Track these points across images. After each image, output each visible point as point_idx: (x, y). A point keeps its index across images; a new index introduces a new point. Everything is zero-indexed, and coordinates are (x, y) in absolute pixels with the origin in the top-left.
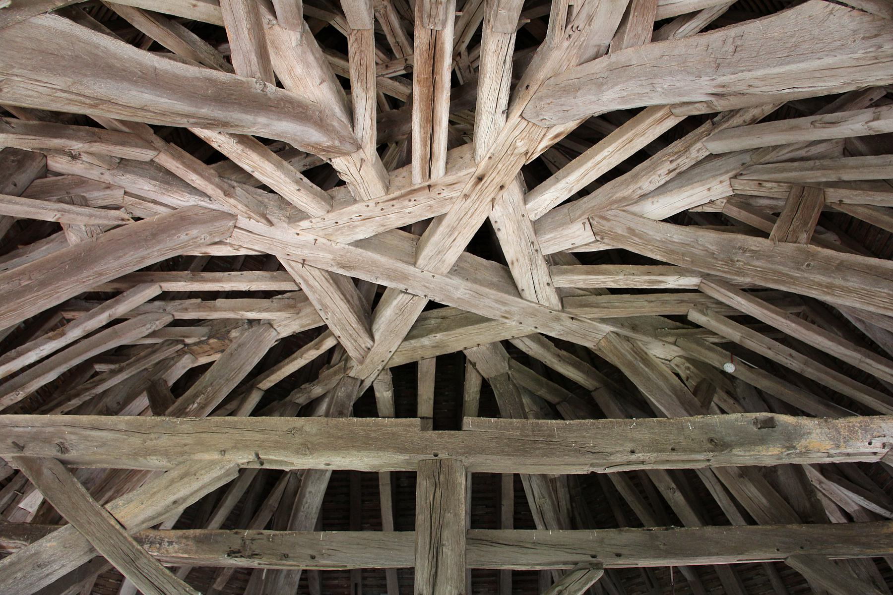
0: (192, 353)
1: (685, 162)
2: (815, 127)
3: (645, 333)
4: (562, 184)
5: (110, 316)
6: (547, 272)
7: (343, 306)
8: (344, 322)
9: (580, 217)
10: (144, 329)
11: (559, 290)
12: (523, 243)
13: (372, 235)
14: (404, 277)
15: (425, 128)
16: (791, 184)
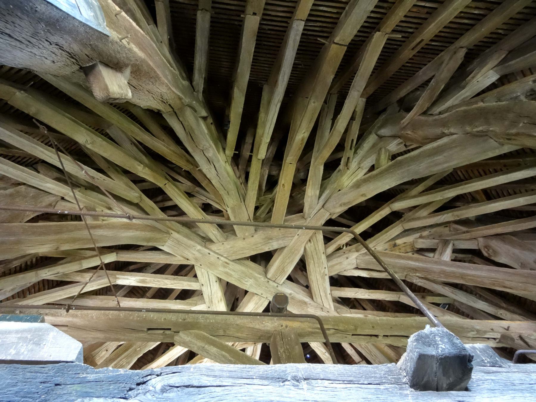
11: (197, 281)
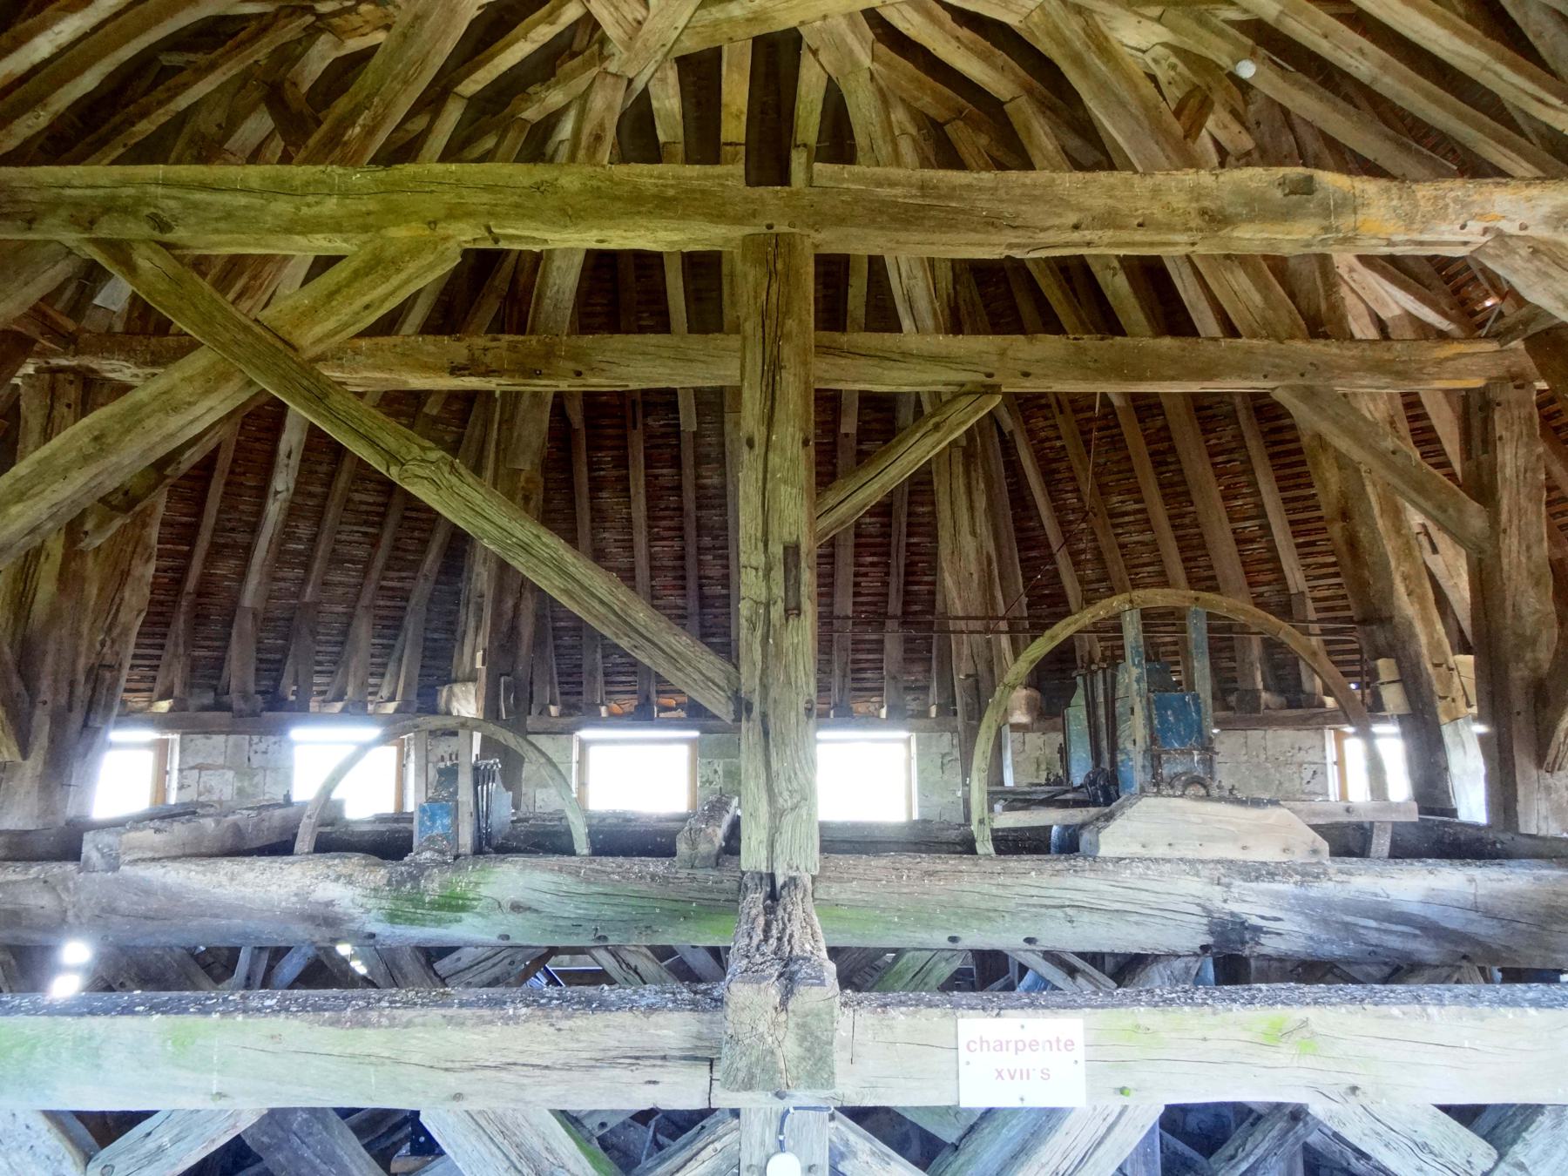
0: (332, 30)
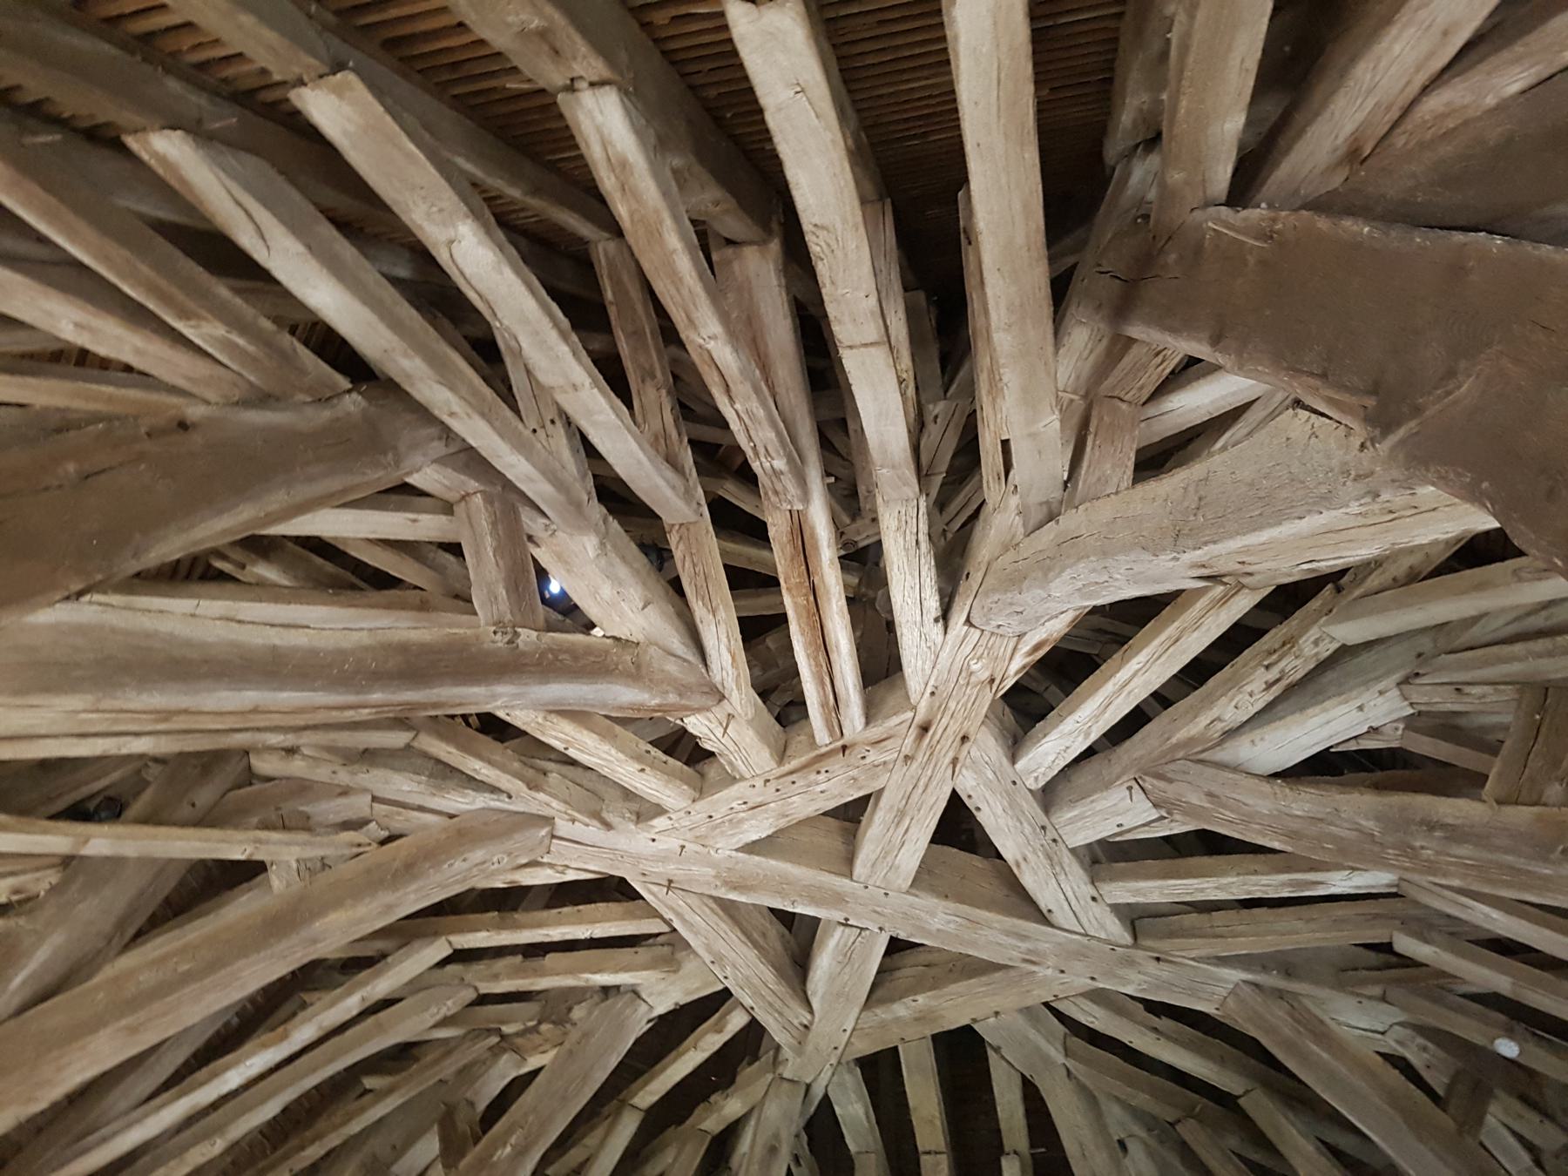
1: (1295, 666)
2: (1520, 580)
3: (1317, 981)
4: (1069, 724)
5: (363, 999)
6: (1086, 878)
7: (751, 954)
8: (756, 981)
9: (1118, 778)
10: (427, 1015)
11: (1116, 909)
12: (1028, 829)
13: (770, 832)
14: (838, 899)
15: (815, 659)
16: (1522, 685)
